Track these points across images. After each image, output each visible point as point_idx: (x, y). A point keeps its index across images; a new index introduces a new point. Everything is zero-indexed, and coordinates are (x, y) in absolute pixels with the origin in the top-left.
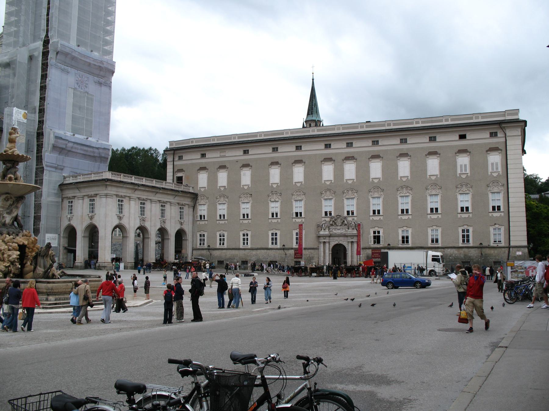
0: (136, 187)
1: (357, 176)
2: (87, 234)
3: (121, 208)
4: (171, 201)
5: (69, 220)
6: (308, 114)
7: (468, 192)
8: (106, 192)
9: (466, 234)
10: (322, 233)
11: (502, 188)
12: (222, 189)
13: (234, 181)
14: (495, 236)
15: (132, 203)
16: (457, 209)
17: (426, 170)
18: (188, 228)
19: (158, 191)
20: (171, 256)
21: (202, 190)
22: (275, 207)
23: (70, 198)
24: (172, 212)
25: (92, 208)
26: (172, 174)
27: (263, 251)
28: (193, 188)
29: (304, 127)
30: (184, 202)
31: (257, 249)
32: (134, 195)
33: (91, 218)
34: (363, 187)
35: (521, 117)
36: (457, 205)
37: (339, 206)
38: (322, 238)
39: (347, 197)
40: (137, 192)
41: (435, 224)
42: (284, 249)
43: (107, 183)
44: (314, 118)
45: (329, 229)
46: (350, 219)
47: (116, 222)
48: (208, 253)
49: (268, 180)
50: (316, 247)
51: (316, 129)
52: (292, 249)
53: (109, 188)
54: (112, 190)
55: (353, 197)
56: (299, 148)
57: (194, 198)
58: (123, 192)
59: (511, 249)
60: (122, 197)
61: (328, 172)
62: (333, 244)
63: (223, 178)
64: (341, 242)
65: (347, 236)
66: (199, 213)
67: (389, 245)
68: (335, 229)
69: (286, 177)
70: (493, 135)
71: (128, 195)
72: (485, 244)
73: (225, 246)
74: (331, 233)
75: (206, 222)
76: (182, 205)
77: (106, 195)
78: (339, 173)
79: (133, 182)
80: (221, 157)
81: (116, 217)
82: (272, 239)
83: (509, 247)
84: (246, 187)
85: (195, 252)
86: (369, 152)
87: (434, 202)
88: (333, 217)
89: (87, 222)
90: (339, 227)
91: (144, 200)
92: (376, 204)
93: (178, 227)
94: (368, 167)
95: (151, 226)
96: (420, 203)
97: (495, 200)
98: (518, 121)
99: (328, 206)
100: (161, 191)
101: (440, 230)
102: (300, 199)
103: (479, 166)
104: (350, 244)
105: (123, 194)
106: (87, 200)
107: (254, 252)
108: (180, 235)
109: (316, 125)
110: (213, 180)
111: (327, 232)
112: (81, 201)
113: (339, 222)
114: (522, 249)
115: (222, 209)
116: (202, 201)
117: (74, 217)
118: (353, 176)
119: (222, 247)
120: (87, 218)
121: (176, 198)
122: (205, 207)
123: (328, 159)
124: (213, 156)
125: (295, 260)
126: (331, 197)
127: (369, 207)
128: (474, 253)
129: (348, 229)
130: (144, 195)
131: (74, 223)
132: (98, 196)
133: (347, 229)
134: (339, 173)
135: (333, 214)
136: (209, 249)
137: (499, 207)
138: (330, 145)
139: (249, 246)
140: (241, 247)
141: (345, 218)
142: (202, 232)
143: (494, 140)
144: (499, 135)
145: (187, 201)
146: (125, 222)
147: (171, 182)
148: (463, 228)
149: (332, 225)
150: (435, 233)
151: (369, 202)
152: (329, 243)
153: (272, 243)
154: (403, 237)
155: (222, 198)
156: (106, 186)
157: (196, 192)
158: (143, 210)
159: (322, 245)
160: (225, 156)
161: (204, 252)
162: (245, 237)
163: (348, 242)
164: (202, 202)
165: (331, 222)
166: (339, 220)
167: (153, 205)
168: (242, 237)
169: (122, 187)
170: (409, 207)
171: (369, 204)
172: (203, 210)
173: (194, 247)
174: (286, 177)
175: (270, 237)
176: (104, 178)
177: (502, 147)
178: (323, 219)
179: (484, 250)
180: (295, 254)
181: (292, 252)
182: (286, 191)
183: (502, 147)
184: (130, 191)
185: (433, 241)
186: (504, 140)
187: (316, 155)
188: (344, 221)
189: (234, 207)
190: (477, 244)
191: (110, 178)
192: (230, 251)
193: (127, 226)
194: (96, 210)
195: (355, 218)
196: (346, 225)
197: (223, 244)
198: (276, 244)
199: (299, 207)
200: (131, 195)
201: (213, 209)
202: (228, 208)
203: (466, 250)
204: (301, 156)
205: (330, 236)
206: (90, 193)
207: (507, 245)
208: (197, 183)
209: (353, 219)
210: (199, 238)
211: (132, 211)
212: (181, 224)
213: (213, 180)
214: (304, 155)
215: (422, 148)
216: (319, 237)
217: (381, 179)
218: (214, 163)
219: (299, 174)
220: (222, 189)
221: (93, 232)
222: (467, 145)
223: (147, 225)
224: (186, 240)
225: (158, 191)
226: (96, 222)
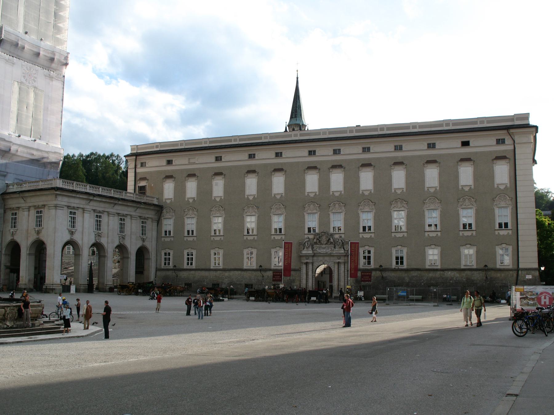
0: (91, 198)
1: (345, 187)
2: (33, 252)
3: (73, 222)
4: (132, 213)
5: (13, 234)
6: (291, 117)
7: (470, 206)
8: (55, 202)
10: (304, 252)
12: (191, 201)
13: (205, 191)
15: (87, 215)
16: (459, 225)
17: (423, 181)
18: (151, 245)
19: (116, 202)
20: (132, 277)
21: (168, 201)
23: (13, 209)
24: (133, 227)
25: (39, 221)
26: (133, 183)
27: (237, 273)
28: (158, 199)
29: (286, 131)
30: (147, 216)
31: (202, 270)
32: (88, 207)
33: (38, 233)
35: (532, 122)
37: (324, 221)
38: (304, 258)
39: (334, 211)
40: (92, 203)
42: (260, 270)
43: (57, 192)
44: (298, 122)
45: (313, 248)
46: (337, 236)
47: (67, 237)
48: (174, 274)
49: (244, 191)
50: (297, 268)
51: (298, 132)
52: (270, 270)
53: (60, 198)
54: (63, 201)
55: (340, 211)
56: (278, 155)
57: (158, 211)
58: (75, 202)
59: (520, 272)
60: (74, 208)
65: (333, 256)
66: (165, 228)
67: (381, 266)
68: (319, 248)
69: (265, 187)
70: (501, 142)
71: (82, 206)
72: (490, 266)
73: (194, 266)
74: (315, 252)
75: (172, 239)
76: (145, 219)
77: (56, 207)
78: (325, 184)
79: (88, 191)
80: (190, 164)
81: (67, 231)
83: (518, 270)
84: (218, 199)
85: (159, 273)
88: (318, 234)
89: (33, 238)
90: (324, 246)
91: (100, 212)
93: (139, 244)
94: (358, 178)
95: (108, 243)
97: (501, 216)
98: (528, 126)
99: (312, 221)
100: (120, 203)
102: (280, 213)
103: (484, 177)
105: (75, 205)
106: (33, 212)
107: (227, 274)
108: (142, 253)
109: (300, 129)
110: (180, 190)
111: (310, 252)
112: (26, 213)
113: (324, 239)
114: (533, 272)
115: (191, 224)
116: (168, 214)
117: (18, 232)
119: (189, 267)
120: (33, 232)
121: (138, 210)
122: (171, 222)
123: (312, 168)
124: (181, 163)
125: (274, 283)
126: (315, 211)
127: (359, 223)
129: (335, 247)
130: (100, 207)
131: (18, 238)
132: (46, 207)
133: (333, 248)
134: (325, 184)
135: (317, 231)
136: (175, 269)
137: (506, 225)
138: (315, 151)
141: (332, 235)
142: (167, 250)
143: (501, 148)
144: (506, 142)
145: (150, 214)
146: (77, 237)
147: (133, 192)
149: (316, 243)
151: (358, 217)
152: (313, 263)
154: (397, 258)
155: (191, 212)
156: (56, 195)
157: (161, 204)
158: (98, 224)
159: (304, 266)
160: (194, 163)
161: (169, 273)
162: (216, 256)
163: (335, 262)
164: (168, 216)
165: (315, 240)
166: (324, 238)
167: (111, 218)
169: (75, 197)
171: (359, 220)
172: (168, 224)
173: (158, 267)
174: (265, 187)
176: (53, 186)
178: (306, 236)
180: (274, 276)
181: (270, 274)
182: (264, 204)
183: (510, 155)
184: (84, 202)
186: (512, 147)
188: (329, 239)
190: (481, 266)
191: (61, 186)
192: (199, 272)
193: (80, 242)
194: (44, 223)
195: (343, 236)
196: (331, 243)
197: (191, 264)
200: (85, 207)
201: (180, 224)
202: (197, 223)
203: (469, 273)
204: (281, 164)
205: (313, 256)
206: (36, 204)
207: (516, 267)
208: (162, 193)
209: (341, 237)
210: (163, 257)
211: (86, 225)
212: (143, 240)
213: (180, 190)
214: (285, 163)
215: (420, 156)
216: (301, 256)
217: (372, 191)
218: (182, 171)
220: (191, 201)
221: (39, 248)
222: (470, 153)
223: (103, 241)
224: (149, 259)
225: (116, 202)
226: (43, 237)
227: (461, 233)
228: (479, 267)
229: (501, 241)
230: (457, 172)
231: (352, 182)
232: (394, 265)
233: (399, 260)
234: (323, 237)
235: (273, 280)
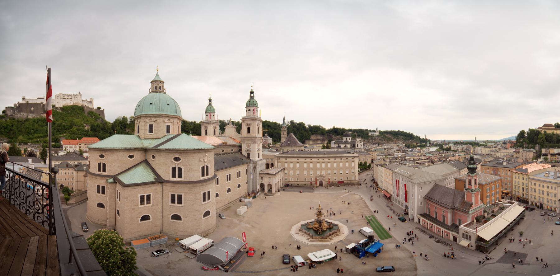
14: (353, 178)
22: (305, 172)
34: (326, 169)
37: (321, 173)
63: (292, 165)
69: (308, 166)
78: (321, 166)
87: (341, 172)
92: (329, 172)
99: (318, 172)
103: (350, 165)
110: (289, 165)
115: (292, 172)
123: (318, 162)
134: (321, 166)
174: (308, 166)
182: (308, 169)
199: (311, 172)
201: (289, 172)
213: (289, 165)
219: (311, 165)
226: (271, 183)
229: (353, 176)
231: (326, 166)
234: (320, 176)
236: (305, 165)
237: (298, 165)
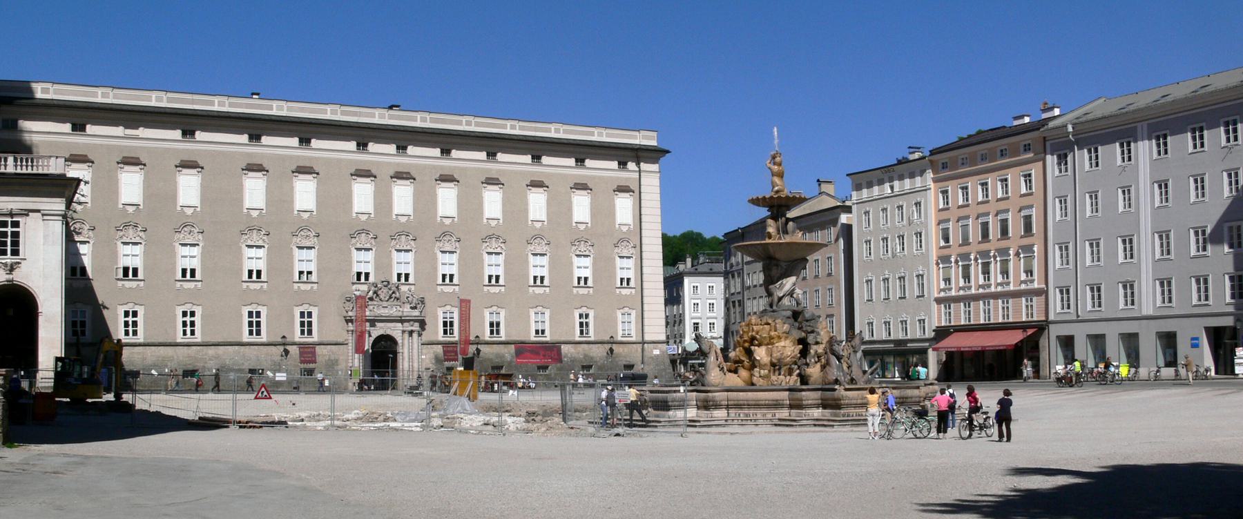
9: (584, 320)
11: (633, 251)
14: (626, 327)
17: (526, 211)
22: (255, 259)
34: (423, 231)
36: (572, 273)
37: (383, 263)
41: (540, 303)
42: (284, 344)
49: (240, 200)
61: (363, 195)
62: (376, 333)
64: (389, 332)
78: (383, 201)
82: (250, 324)
83: (643, 343)
86: (434, 167)
90: (385, 304)
96: (516, 266)
101: (547, 313)
103: (603, 212)
104: (406, 335)
107: (211, 351)
118: (409, 210)
125: (303, 366)
126: (368, 246)
127: (435, 269)
128: (598, 352)
134: (383, 201)
135: (372, 279)
139: (198, 338)
140: (179, 340)
148: (581, 311)
149: (371, 299)
150: (540, 318)
151: (435, 259)
153: (251, 333)
165: (371, 294)
168: (180, 319)
170: (500, 271)
174: (280, 198)
175: (246, 319)
177: (634, 186)
179: (614, 347)
180: (301, 354)
182: (279, 226)
185: (537, 332)
187: (339, 161)
189: (159, 252)
198: (258, 333)
199: (305, 260)
215: (521, 173)
227: (439, 288)
228: (600, 338)
229: (623, 304)
230: (571, 203)
231: (425, 202)
232: (487, 336)
233: (495, 327)
234: (390, 289)
235: (302, 362)
236: (255, 191)
237: (189, 188)
